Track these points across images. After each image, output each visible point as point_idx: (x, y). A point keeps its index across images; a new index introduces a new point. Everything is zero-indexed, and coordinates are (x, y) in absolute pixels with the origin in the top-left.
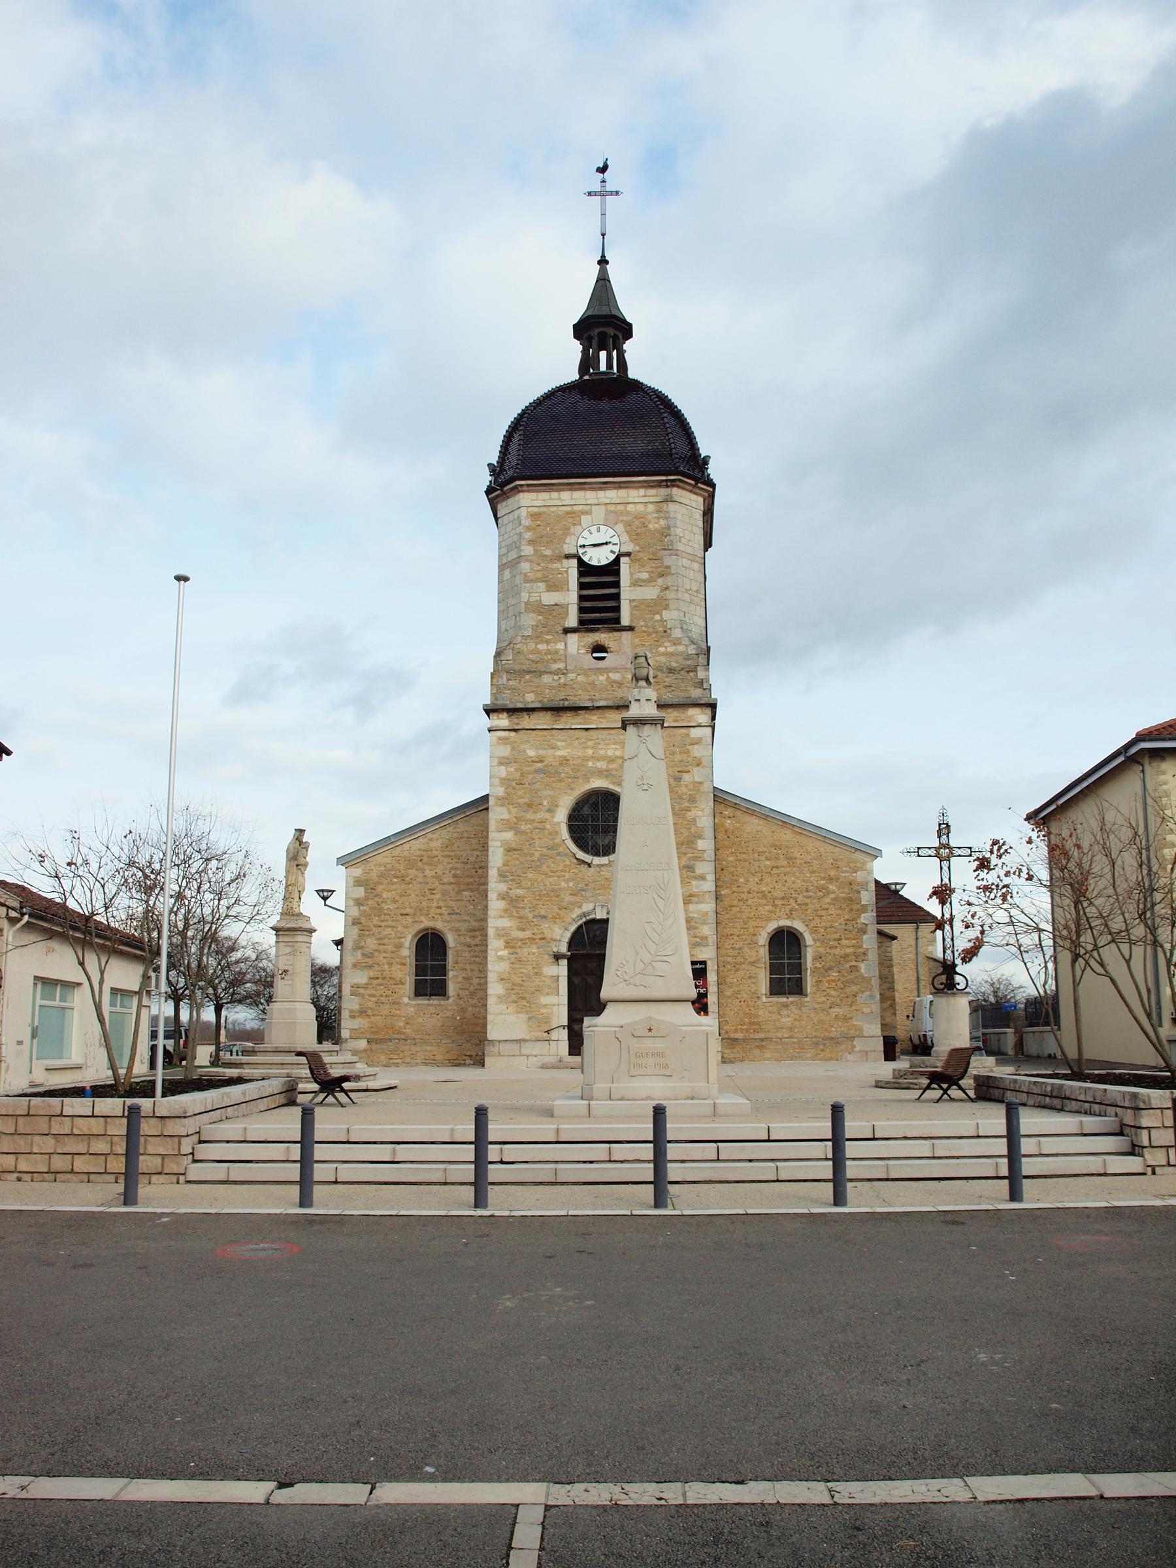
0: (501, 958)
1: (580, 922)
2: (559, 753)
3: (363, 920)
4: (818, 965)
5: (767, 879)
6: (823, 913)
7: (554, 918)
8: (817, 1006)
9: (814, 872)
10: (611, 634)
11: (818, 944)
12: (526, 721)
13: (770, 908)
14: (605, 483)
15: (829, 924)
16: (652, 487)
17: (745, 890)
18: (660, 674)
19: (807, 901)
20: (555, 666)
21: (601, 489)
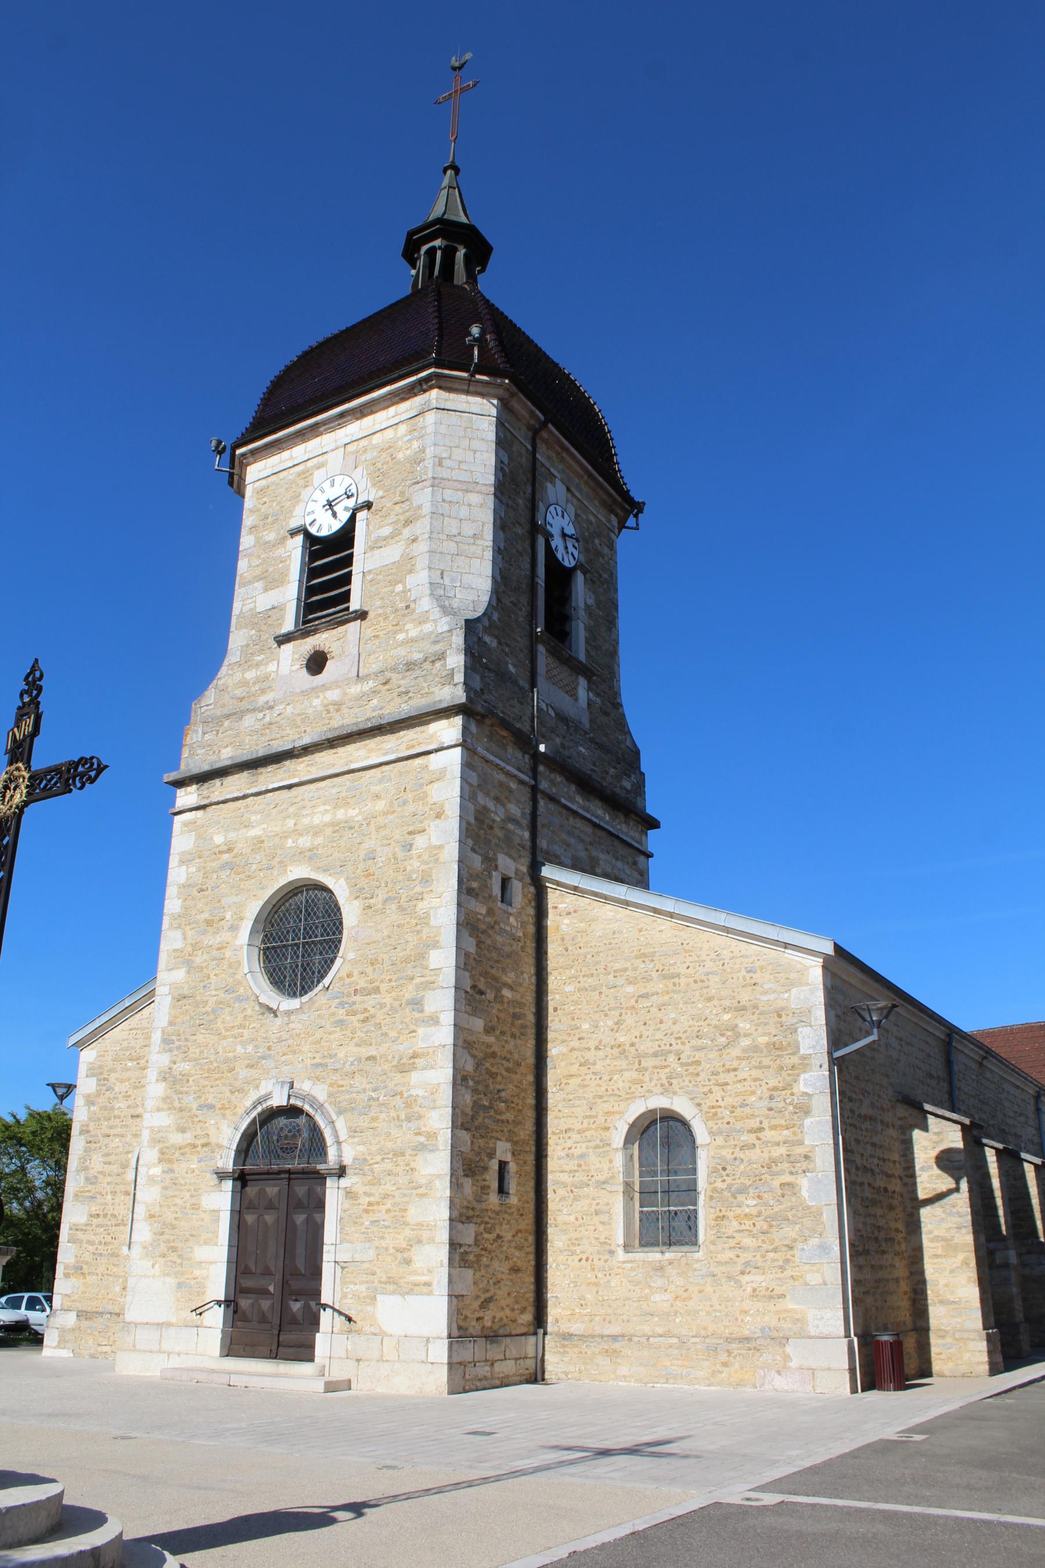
0: (152, 1180)
1: (254, 1114)
2: (253, 833)
3: (92, 1127)
4: (719, 1185)
5: (629, 1020)
6: (729, 1077)
7: (223, 1108)
8: (718, 1270)
9: (710, 999)
10: (334, 632)
11: (720, 1140)
12: (218, 789)
13: (634, 1075)
14: (342, 415)
15: (740, 1099)
16: (404, 399)
17: (592, 1044)
18: (394, 676)
19: (699, 1056)
20: (262, 700)
21: (340, 426)
